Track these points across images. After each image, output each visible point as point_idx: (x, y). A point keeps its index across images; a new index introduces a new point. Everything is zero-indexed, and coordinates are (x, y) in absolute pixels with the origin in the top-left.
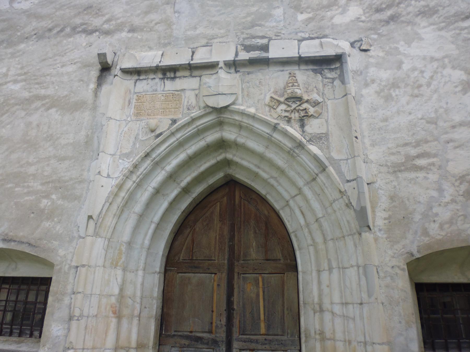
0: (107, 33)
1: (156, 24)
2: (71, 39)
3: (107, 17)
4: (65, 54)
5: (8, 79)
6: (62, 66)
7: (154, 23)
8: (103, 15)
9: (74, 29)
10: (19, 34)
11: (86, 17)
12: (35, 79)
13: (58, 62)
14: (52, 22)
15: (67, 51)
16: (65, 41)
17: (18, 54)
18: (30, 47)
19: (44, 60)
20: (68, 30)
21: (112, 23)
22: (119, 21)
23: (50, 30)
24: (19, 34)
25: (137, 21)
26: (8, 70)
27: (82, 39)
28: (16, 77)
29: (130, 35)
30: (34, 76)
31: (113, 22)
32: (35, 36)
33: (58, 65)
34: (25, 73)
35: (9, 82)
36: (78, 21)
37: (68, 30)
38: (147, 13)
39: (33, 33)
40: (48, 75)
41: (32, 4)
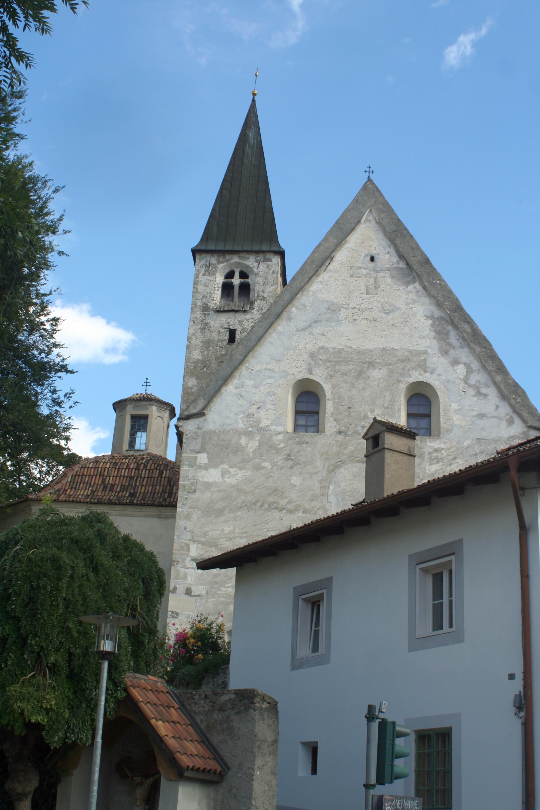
0: (291, 512)
1: (318, 509)
2: (269, 513)
3: (288, 499)
4: (268, 523)
5: (236, 535)
6: (268, 531)
7: (317, 508)
8: (286, 498)
9: (270, 505)
10: (234, 503)
11: (276, 498)
12: (253, 537)
13: (264, 527)
14: (254, 497)
15: (268, 521)
16: (266, 514)
17: (238, 519)
18: (245, 515)
19: (255, 525)
20: (266, 506)
21: (292, 504)
22: (296, 503)
23: (255, 504)
24: (234, 503)
25: (307, 506)
26: (234, 529)
27: (276, 514)
28: (241, 534)
29: (304, 515)
30: (252, 535)
31: (292, 504)
32: (246, 507)
33: (265, 530)
34: (245, 533)
35: (237, 537)
36: (270, 499)
37: (266, 506)
38: (312, 500)
39: (244, 504)
40: (260, 535)
41: (237, 480)
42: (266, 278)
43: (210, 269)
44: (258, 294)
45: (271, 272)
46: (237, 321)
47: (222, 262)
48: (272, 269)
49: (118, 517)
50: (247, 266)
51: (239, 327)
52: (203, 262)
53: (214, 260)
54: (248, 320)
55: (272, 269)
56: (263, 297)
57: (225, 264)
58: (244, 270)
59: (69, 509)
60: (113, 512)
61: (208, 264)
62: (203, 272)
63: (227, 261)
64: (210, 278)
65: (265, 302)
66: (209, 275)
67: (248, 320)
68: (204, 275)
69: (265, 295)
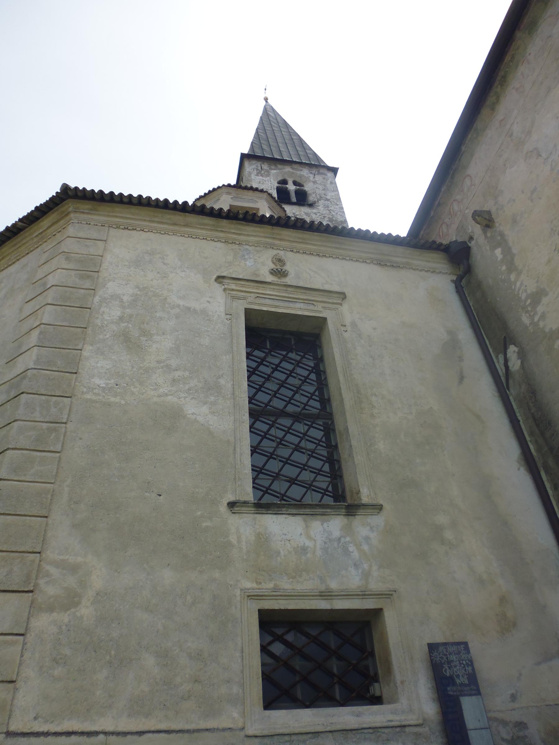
42: (325, 186)
43: (263, 172)
44: (320, 196)
45: (329, 182)
46: (303, 213)
47: (274, 169)
48: (330, 180)
49: (290, 254)
50: (301, 176)
51: (307, 217)
52: (254, 166)
53: (265, 166)
54: (316, 214)
55: (330, 180)
56: (326, 198)
57: (278, 171)
58: (298, 180)
59: (171, 227)
60: (277, 242)
61: (259, 168)
62: (256, 174)
63: (279, 169)
64: (264, 178)
65: (329, 202)
66: (262, 176)
67: (316, 214)
68: (257, 175)
69: (328, 197)
